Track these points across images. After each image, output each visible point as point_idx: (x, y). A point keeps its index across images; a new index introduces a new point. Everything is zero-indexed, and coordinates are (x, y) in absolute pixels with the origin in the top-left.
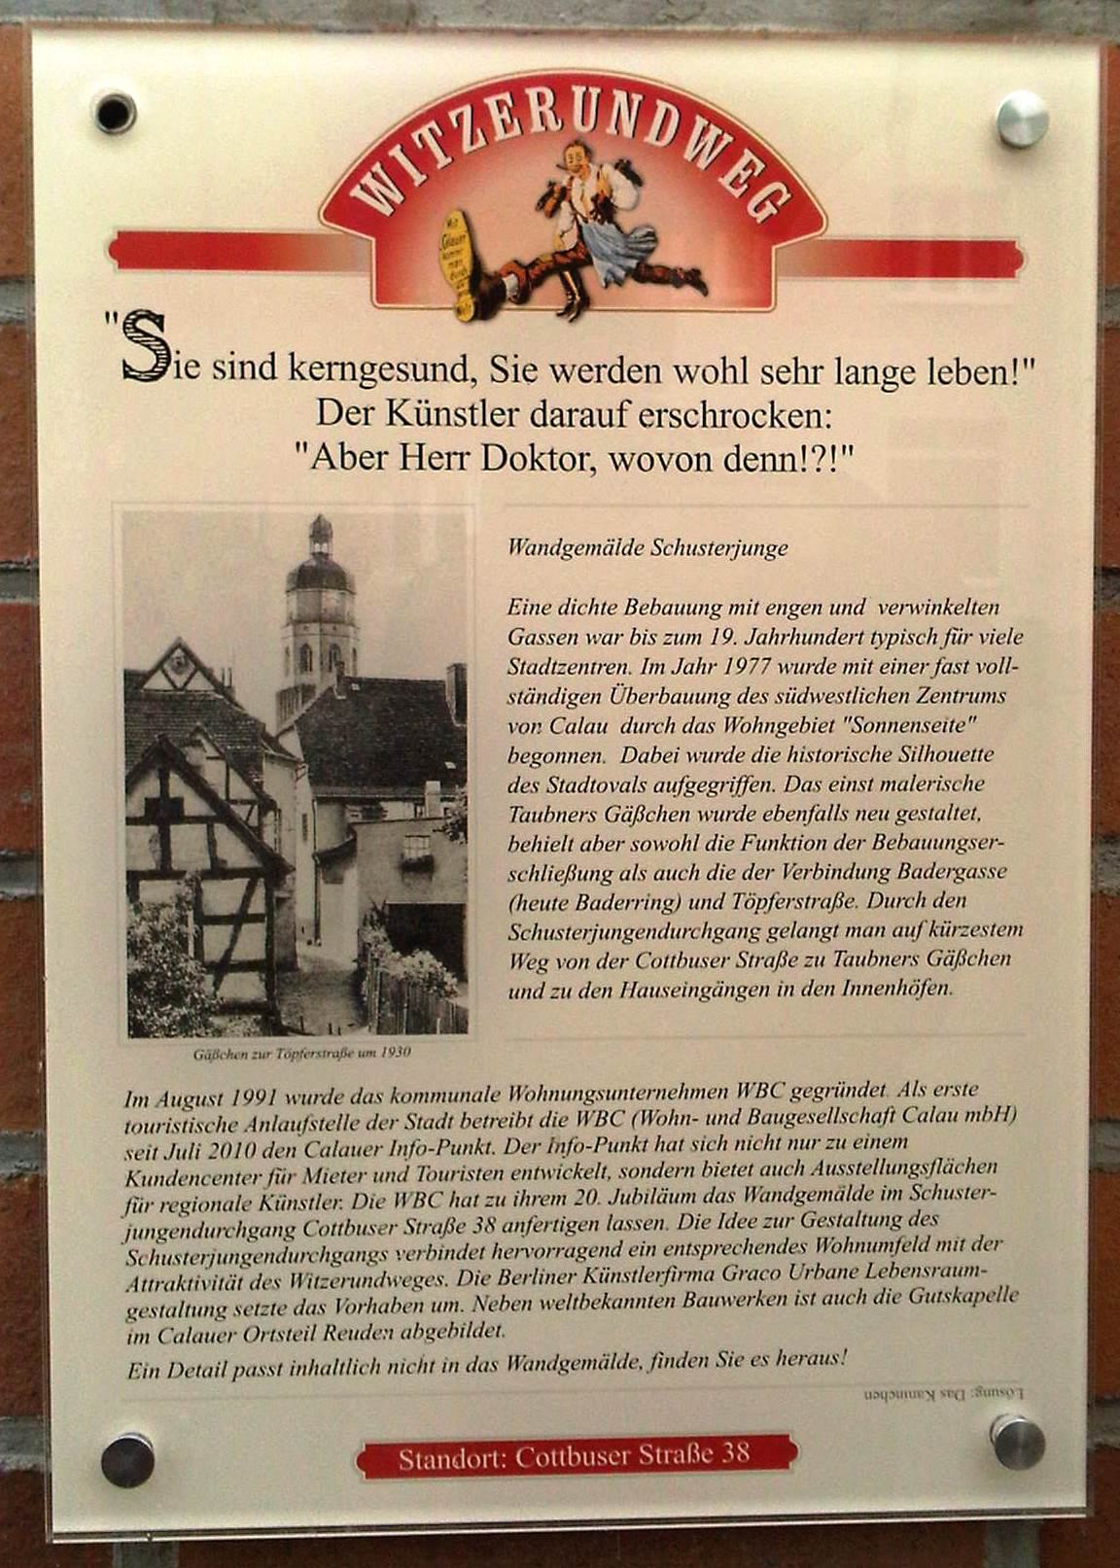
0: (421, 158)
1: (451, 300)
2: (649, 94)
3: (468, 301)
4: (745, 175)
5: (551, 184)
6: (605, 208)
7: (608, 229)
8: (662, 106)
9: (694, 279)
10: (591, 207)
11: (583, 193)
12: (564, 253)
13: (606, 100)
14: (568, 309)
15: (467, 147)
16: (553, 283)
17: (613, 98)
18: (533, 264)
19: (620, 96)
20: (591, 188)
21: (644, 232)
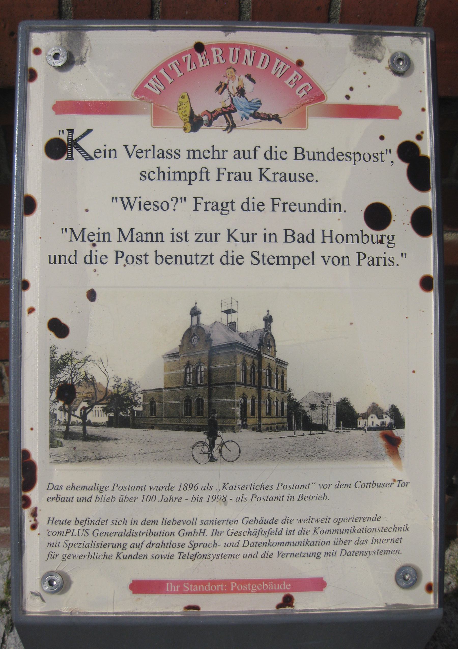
0: (171, 73)
1: (182, 124)
2: (258, 51)
3: (189, 125)
4: (294, 80)
5: (221, 83)
6: (241, 92)
7: (242, 99)
8: (263, 55)
9: (276, 118)
10: (236, 91)
11: (233, 86)
12: (226, 108)
13: (241, 53)
14: (227, 129)
15: (189, 69)
16: (222, 118)
17: (245, 52)
18: (214, 112)
19: (247, 51)
20: (236, 84)
21: (257, 100)
